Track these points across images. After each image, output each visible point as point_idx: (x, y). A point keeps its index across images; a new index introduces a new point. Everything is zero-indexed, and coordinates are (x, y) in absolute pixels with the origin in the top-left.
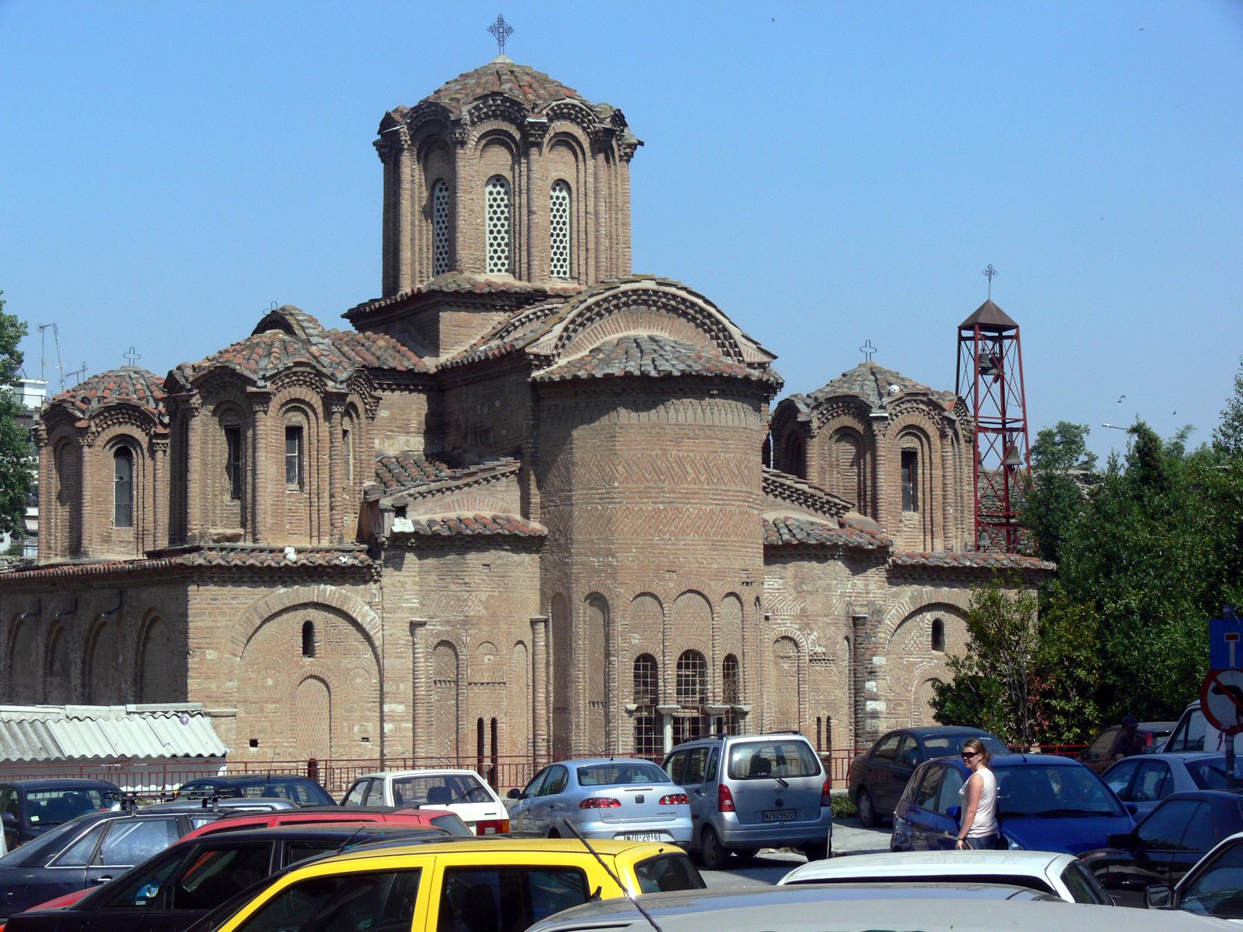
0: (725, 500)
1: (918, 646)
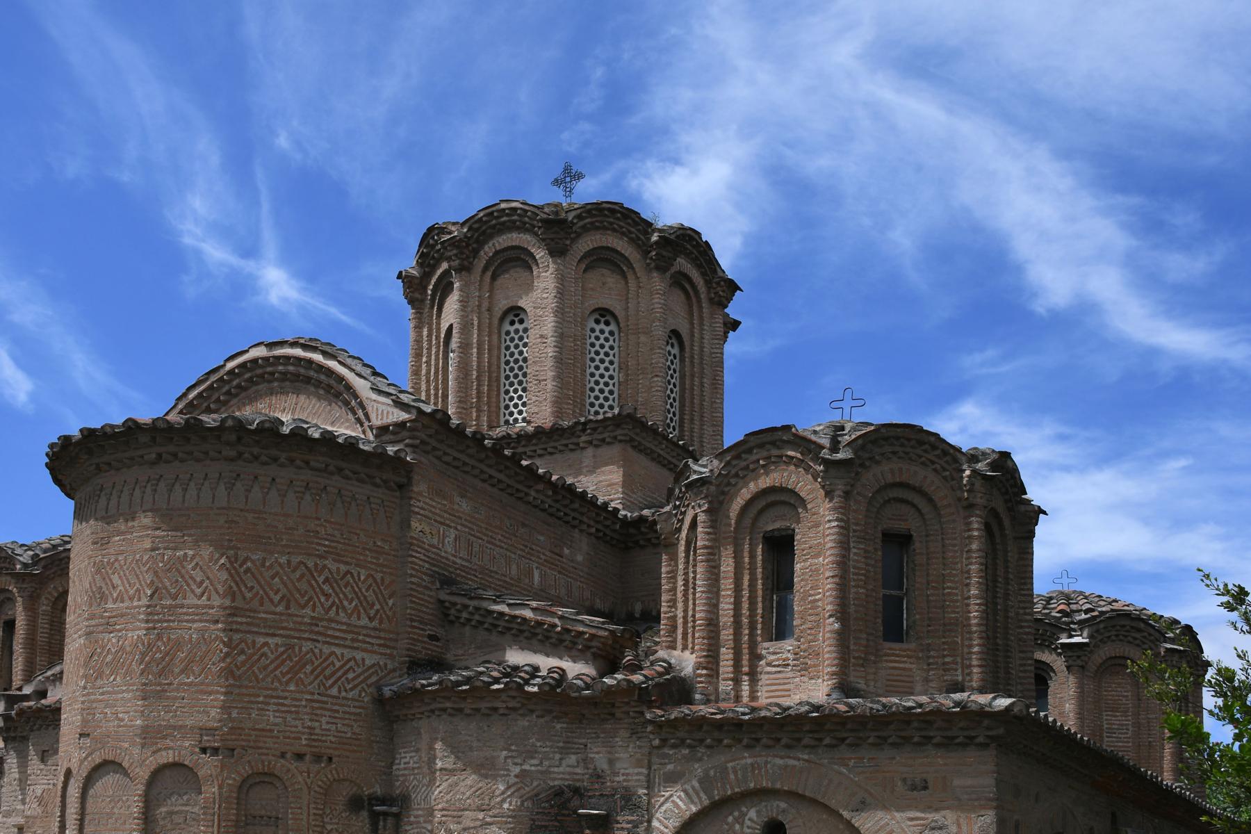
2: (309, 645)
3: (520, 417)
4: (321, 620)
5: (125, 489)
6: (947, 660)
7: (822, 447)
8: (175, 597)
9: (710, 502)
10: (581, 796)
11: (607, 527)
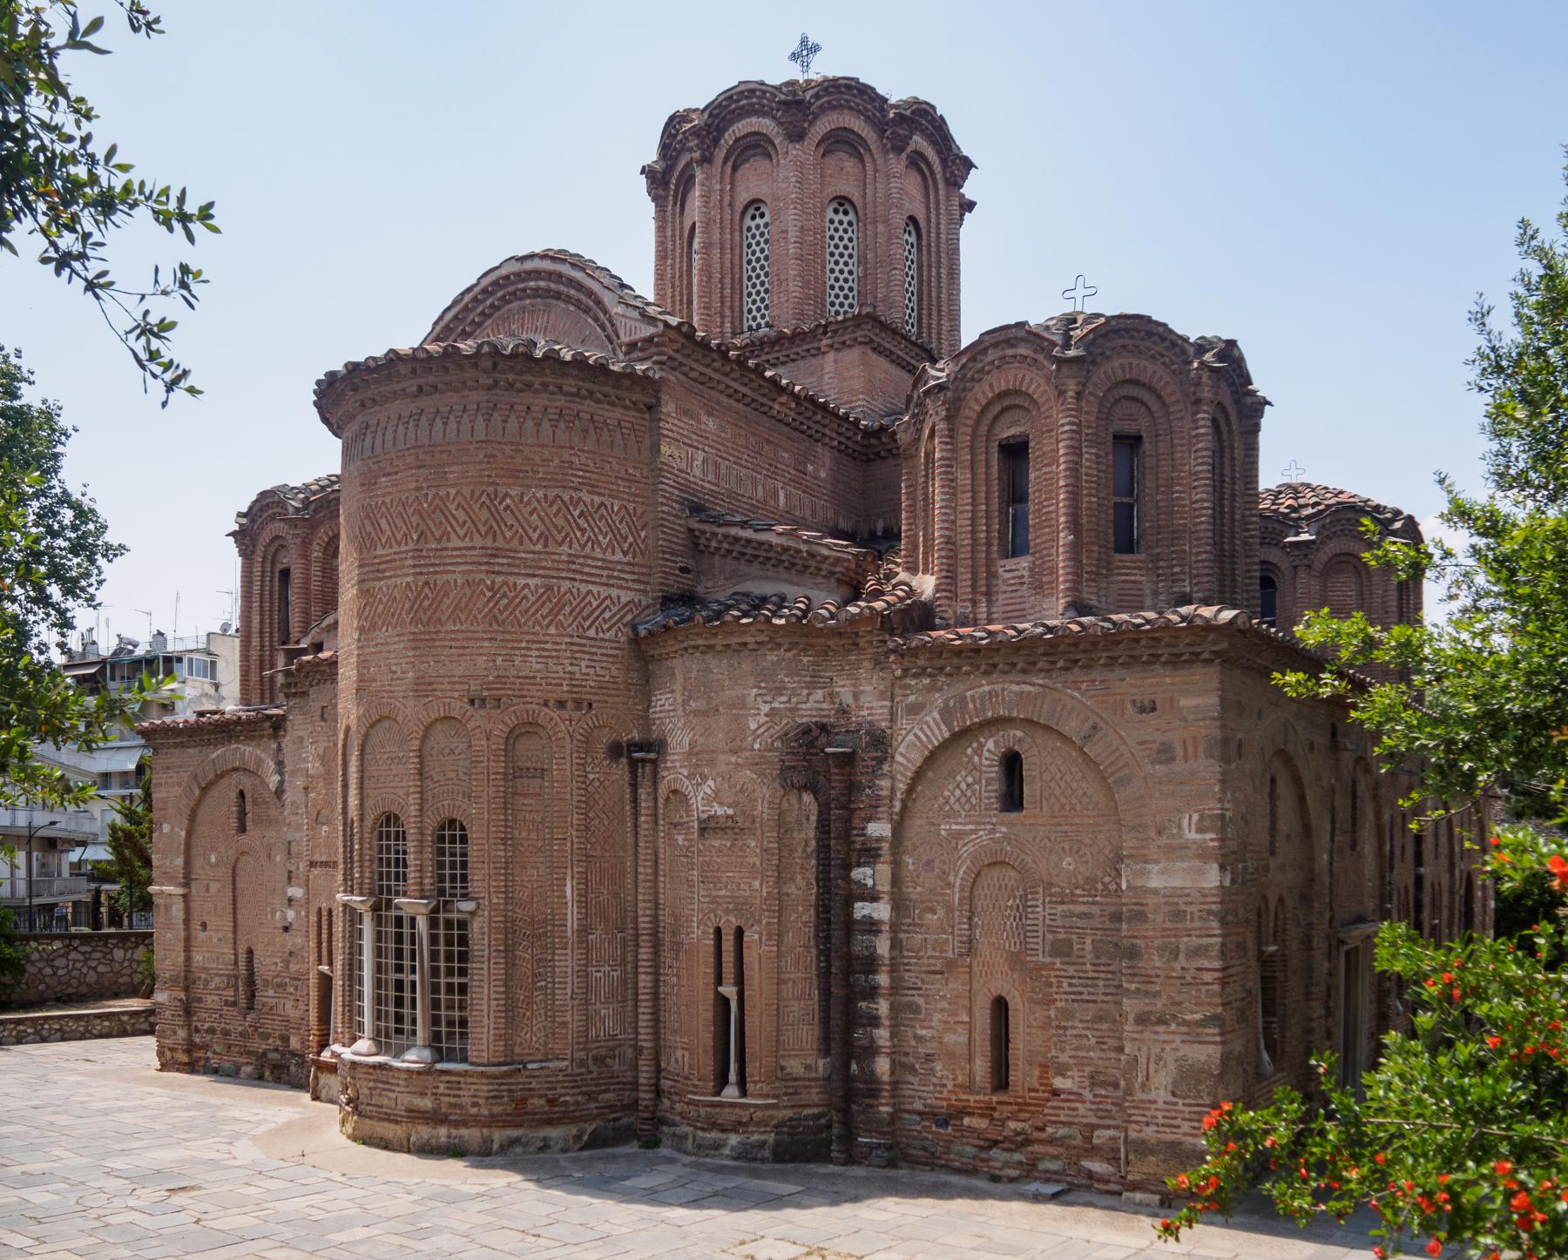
0: (435, 565)
1: (968, 801)
2: (567, 584)
3: (763, 322)
4: (578, 557)
5: (389, 425)
6: (1176, 570)
7: (1054, 344)
8: (439, 541)
9: (947, 409)
10: (828, 733)
11: (849, 438)
